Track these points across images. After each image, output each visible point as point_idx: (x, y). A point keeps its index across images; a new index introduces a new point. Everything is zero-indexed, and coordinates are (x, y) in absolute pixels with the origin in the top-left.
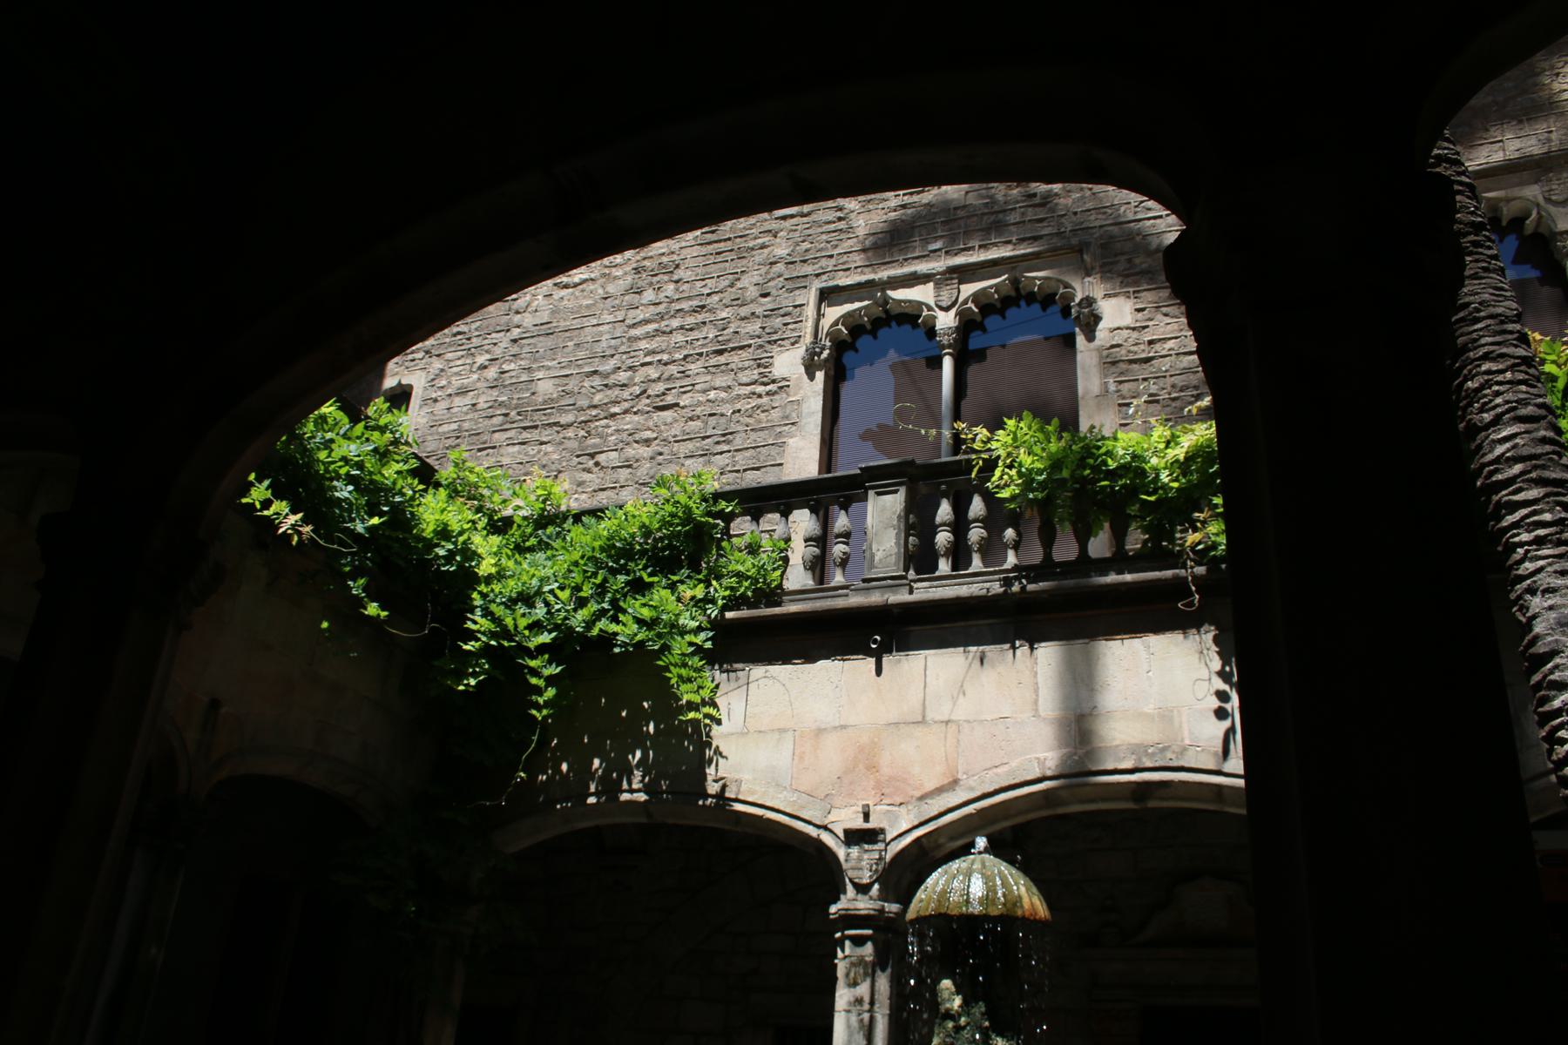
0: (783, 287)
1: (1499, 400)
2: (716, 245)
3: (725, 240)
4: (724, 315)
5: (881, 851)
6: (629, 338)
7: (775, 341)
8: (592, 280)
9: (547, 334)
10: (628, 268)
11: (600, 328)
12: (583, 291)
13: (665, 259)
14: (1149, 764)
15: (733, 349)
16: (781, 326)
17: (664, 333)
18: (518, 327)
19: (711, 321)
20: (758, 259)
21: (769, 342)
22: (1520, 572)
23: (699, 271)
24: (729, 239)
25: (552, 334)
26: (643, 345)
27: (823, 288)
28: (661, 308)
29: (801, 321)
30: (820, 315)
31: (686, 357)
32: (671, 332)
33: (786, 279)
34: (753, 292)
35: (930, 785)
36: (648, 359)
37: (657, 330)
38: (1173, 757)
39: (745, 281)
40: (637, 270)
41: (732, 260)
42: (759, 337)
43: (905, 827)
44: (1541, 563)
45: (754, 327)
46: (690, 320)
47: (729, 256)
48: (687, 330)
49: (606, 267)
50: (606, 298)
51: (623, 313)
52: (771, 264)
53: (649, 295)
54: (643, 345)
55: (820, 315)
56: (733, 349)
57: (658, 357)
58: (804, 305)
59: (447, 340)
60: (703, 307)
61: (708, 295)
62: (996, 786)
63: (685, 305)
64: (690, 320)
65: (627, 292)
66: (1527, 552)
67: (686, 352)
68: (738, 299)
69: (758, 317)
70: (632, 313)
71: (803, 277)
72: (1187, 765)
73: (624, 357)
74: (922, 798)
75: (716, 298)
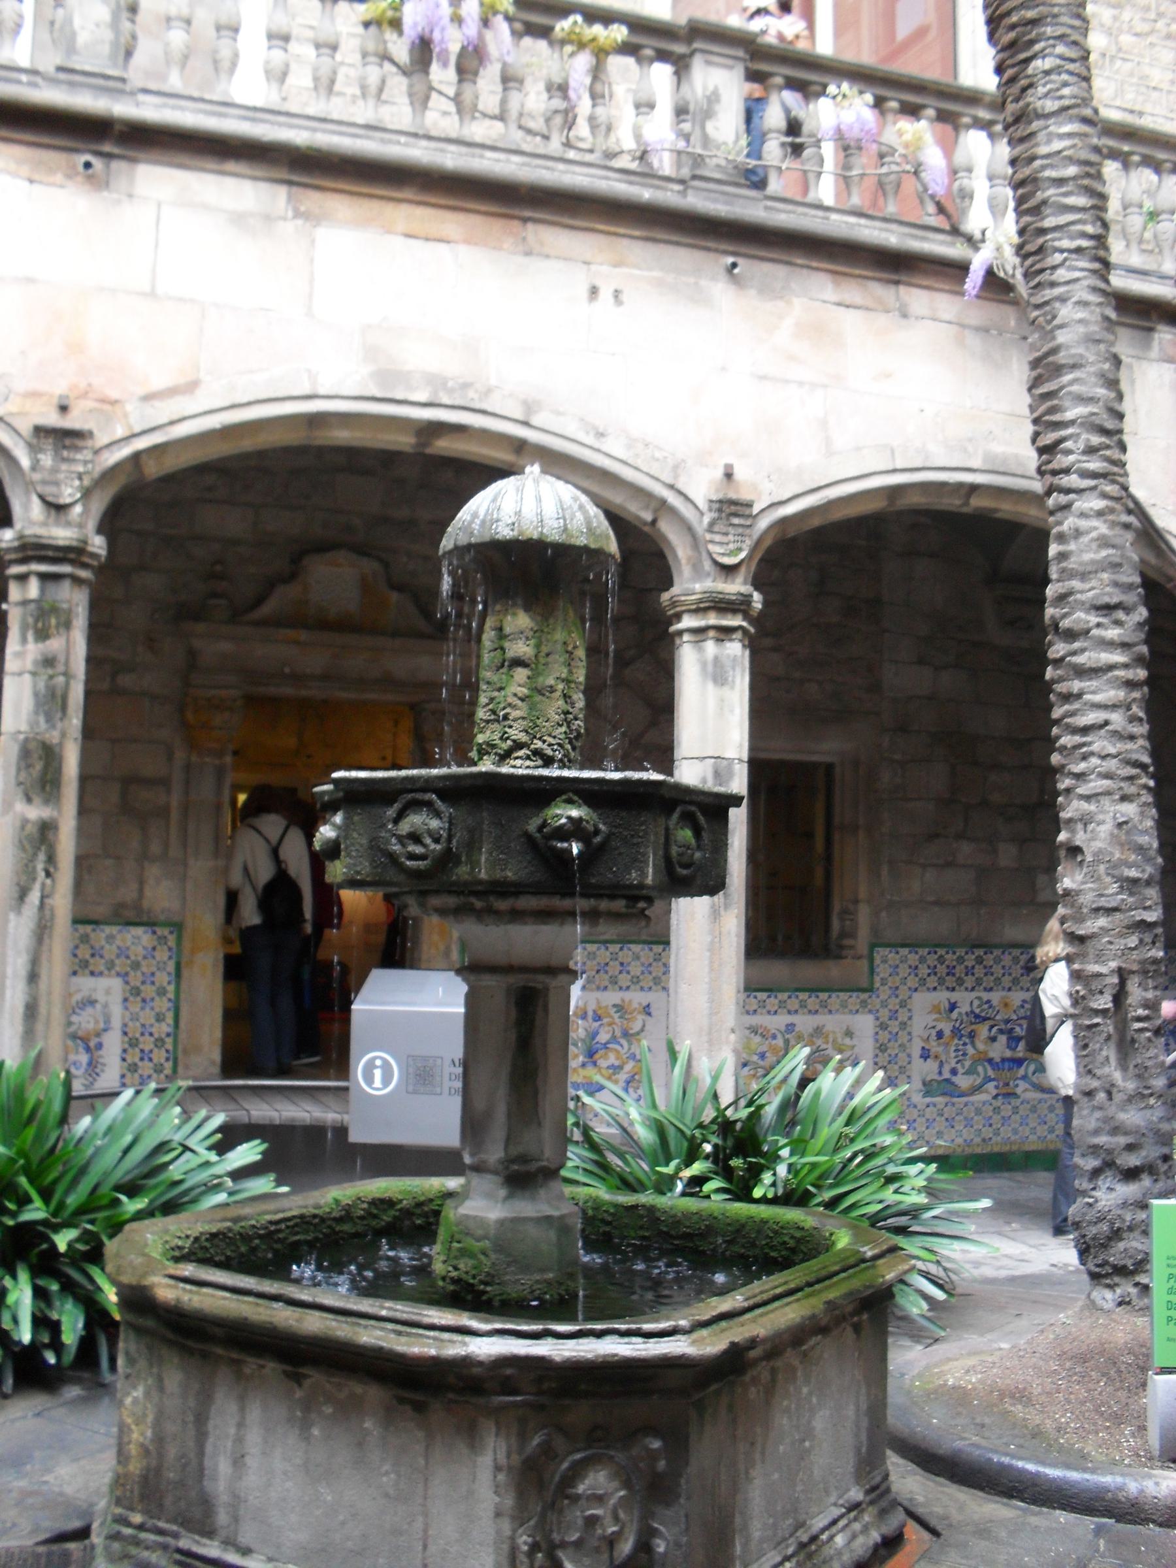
1: (1066, 91)
5: (86, 462)
14: (446, 400)
22: (1054, 277)
35: (159, 382)
38: (476, 396)
44: (1077, 274)
62: (251, 398)
66: (1065, 260)
72: (490, 409)
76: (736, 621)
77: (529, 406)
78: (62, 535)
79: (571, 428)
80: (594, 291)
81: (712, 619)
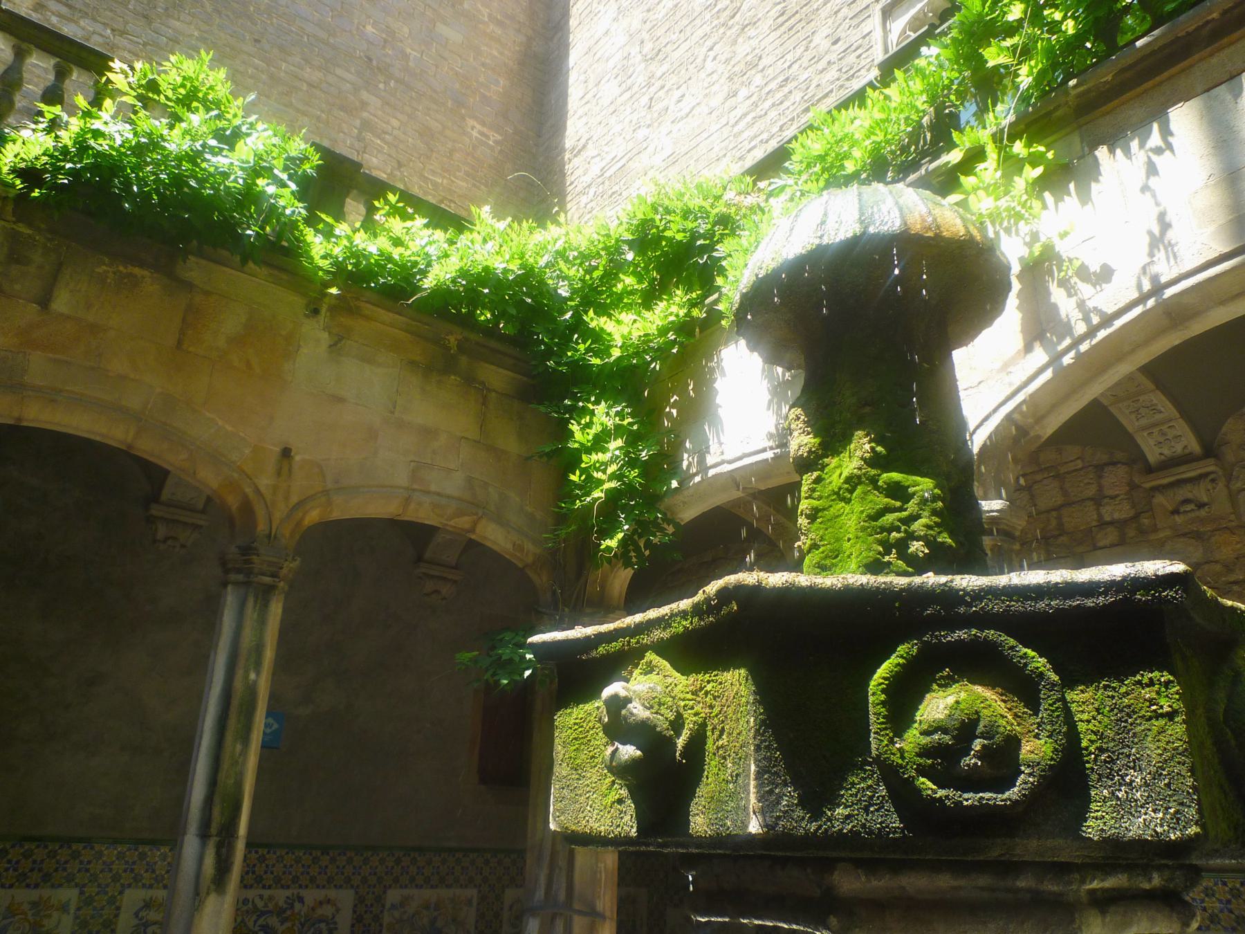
0: (850, 26)
2: (787, 24)
3: (794, 15)
4: (805, 76)
6: (735, 135)
7: (853, 76)
8: (698, 104)
9: (674, 163)
10: (723, 80)
11: (710, 139)
12: (693, 117)
13: (749, 58)
15: (819, 101)
16: (855, 60)
17: (760, 117)
18: (652, 168)
19: (796, 87)
20: (823, 15)
21: (848, 79)
23: (777, 52)
24: (797, 12)
25: (677, 161)
26: (746, 135)
27: (884, 7)
28: (754, 98)
29: (872, 47)
30: (886, 32)
31: (781, 127)
32: (766, 114)
33: (851, 19)
34: (826, 44)
36: (753, 144)
37: (754, 118)
39: (817, 39)
40: (730, 79)
41: (802, 28)
42: (838, 79)
45: (833, 73)
46: (779, 95)
47: (799, 26)
48: (778, 105)
49: (706, 88)
50: (711, 113)
51: (726, 117)
52: (836, 13)
53: (743, 92)
54: (746, 135)
55: (886, 32)
56: (819, 101)
57: (759, 139)
58: (871, 32)
59: (606, 203)
60: (786, 80)
61: (789, 67)
63: (773, 85)
64: (779, 95)
65: (726, 99)
67: (781, 123)
68: (815, 57)
69: (834, 63)
70: (733, 113)
71: (865, 8)
73: (734, 152)
75: (795, 66)
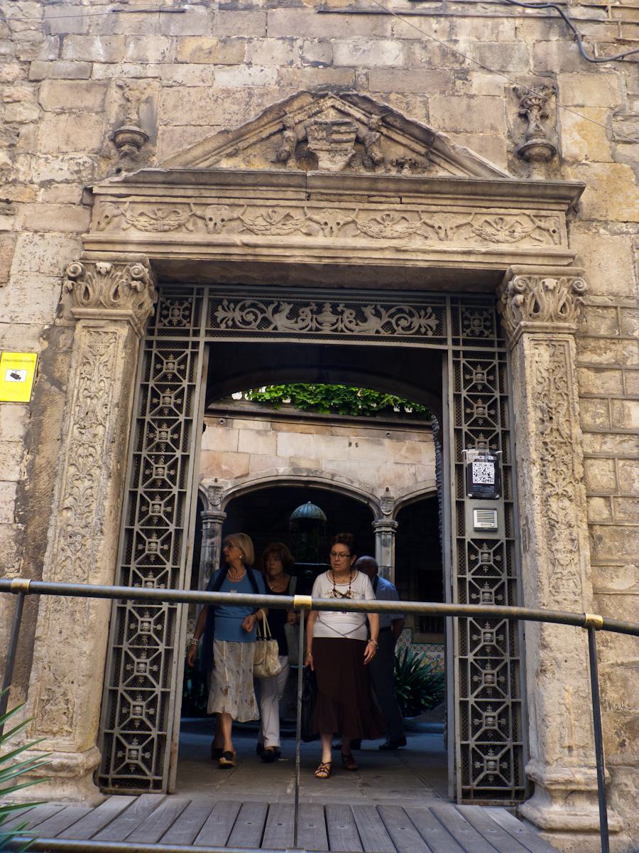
43: (230, 486)
74: (237, 478)
76: (390, 529)
77: (333, 475)
78: (216, 513)
79: (344, 481)
80: (350, 444)
81: (383, 529)
